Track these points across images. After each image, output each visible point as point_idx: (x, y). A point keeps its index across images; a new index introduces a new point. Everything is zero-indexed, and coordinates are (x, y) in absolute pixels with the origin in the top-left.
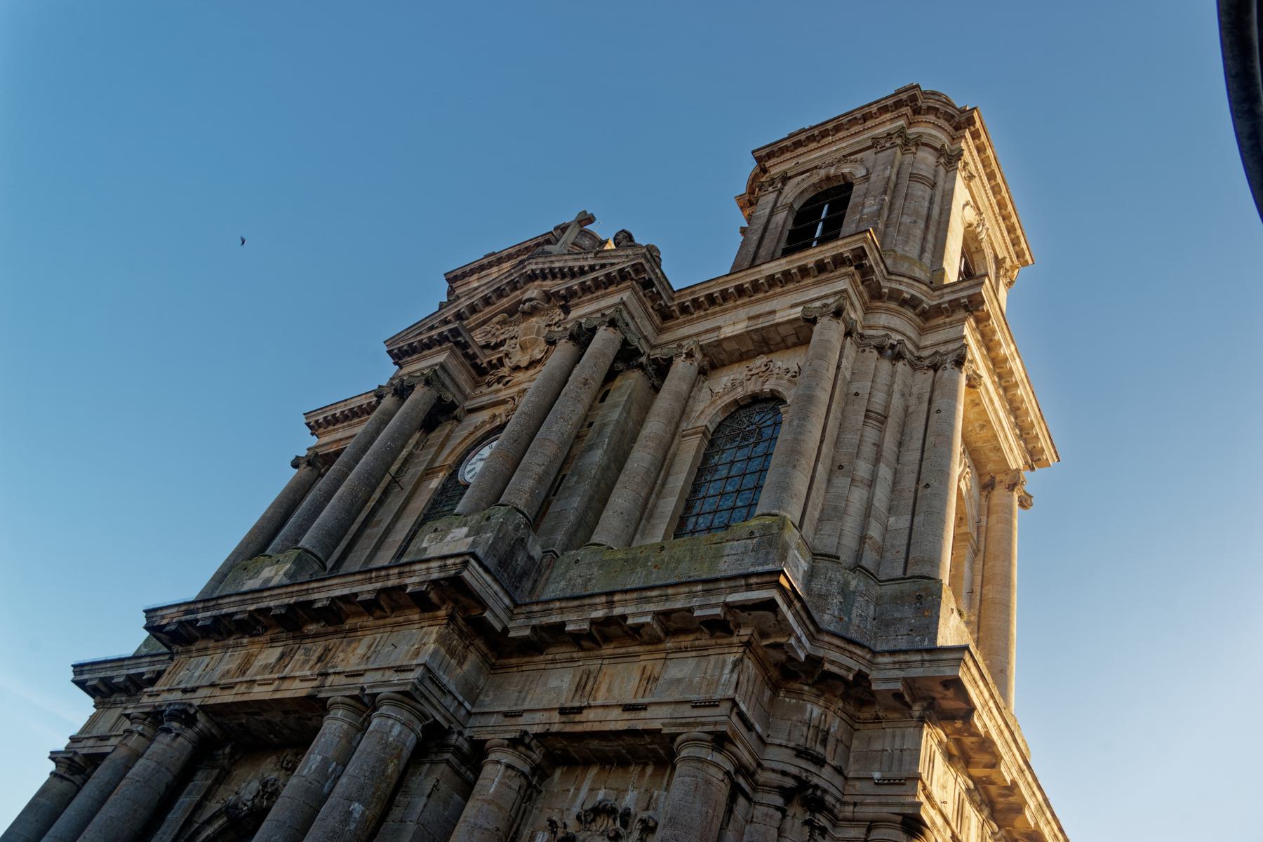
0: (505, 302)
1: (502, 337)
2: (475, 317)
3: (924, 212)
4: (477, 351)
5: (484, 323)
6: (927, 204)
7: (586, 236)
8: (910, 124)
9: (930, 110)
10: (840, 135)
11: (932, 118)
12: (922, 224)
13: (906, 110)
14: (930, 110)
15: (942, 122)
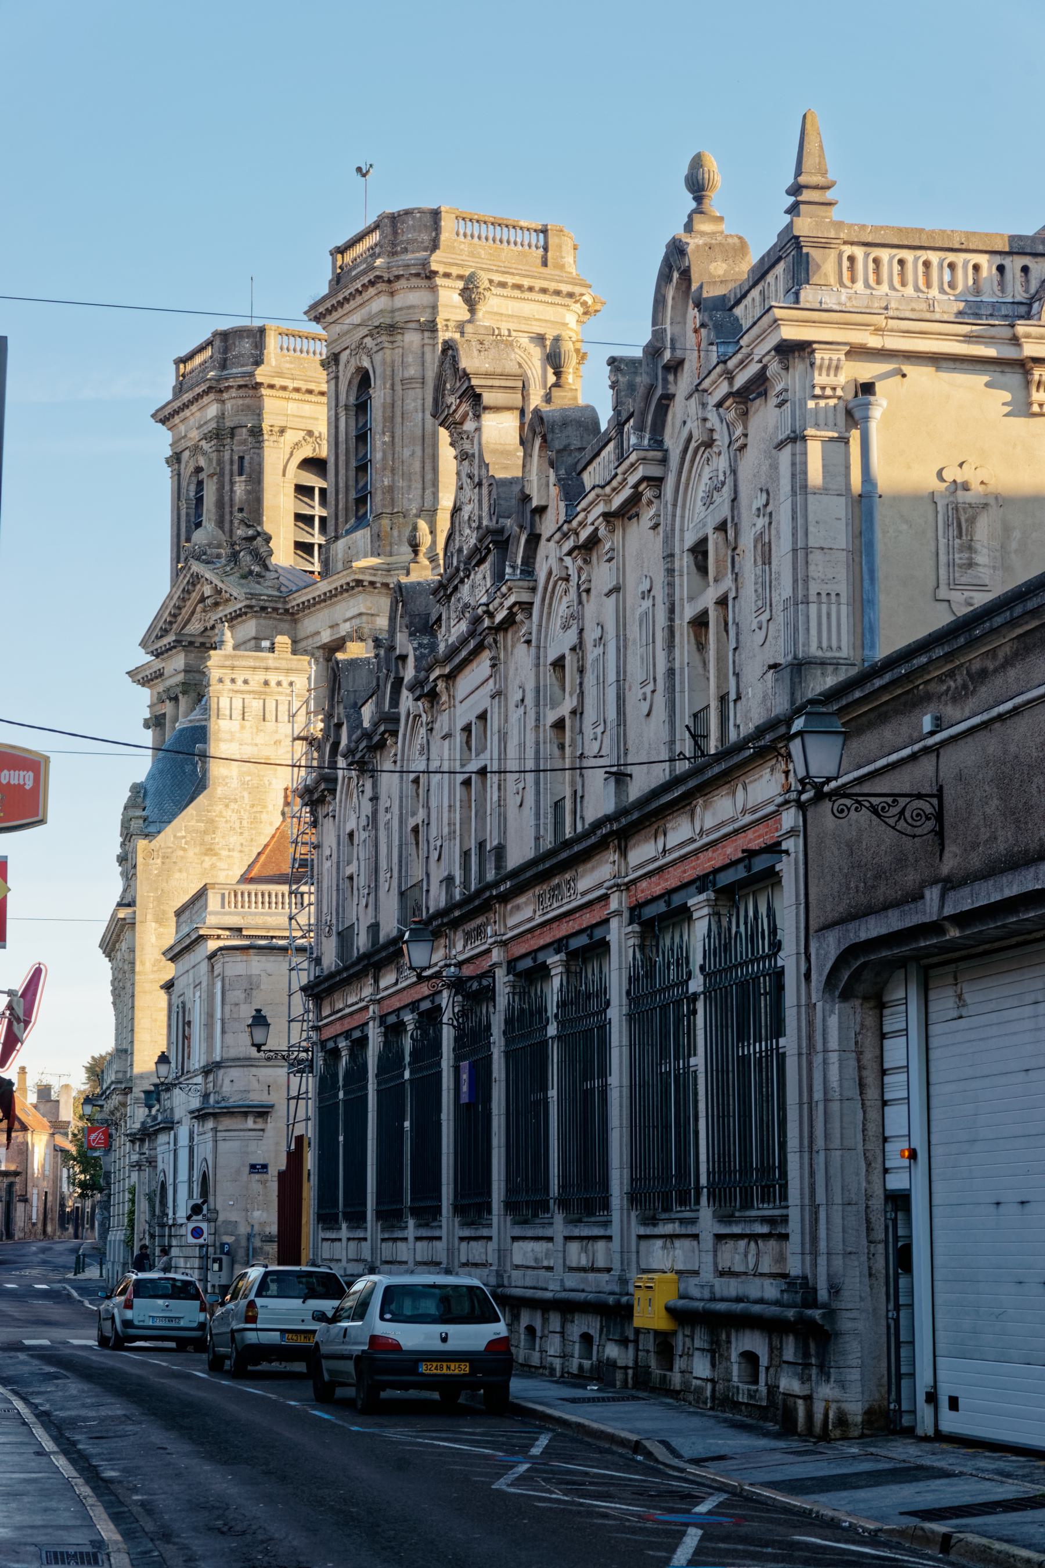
0: (195, 596)
1: (212, 622)
2: (184, 611)
3: (419, 432)
4: (201, 640)
5: (193, 613)
6: (420, 415)
7: (241, 337)
8: (392, 294)
9: (398, 277)
10: (353, 304)
11: (403, 283)
12: (419, 453)
13: (381, 286)
14: (398, 277)
15: (415, 282)
